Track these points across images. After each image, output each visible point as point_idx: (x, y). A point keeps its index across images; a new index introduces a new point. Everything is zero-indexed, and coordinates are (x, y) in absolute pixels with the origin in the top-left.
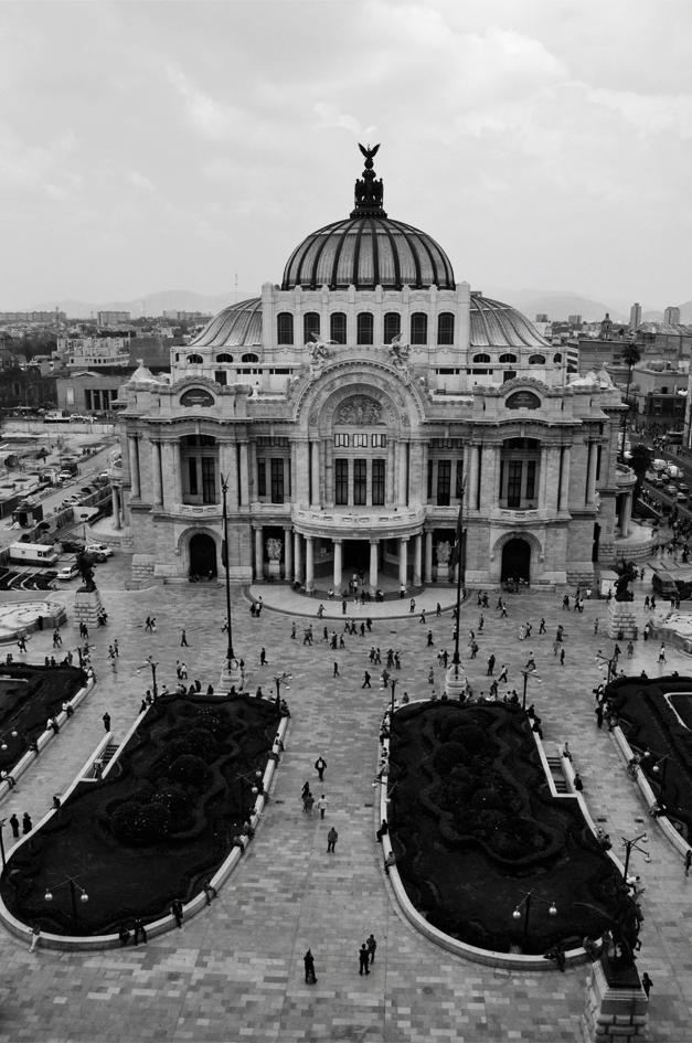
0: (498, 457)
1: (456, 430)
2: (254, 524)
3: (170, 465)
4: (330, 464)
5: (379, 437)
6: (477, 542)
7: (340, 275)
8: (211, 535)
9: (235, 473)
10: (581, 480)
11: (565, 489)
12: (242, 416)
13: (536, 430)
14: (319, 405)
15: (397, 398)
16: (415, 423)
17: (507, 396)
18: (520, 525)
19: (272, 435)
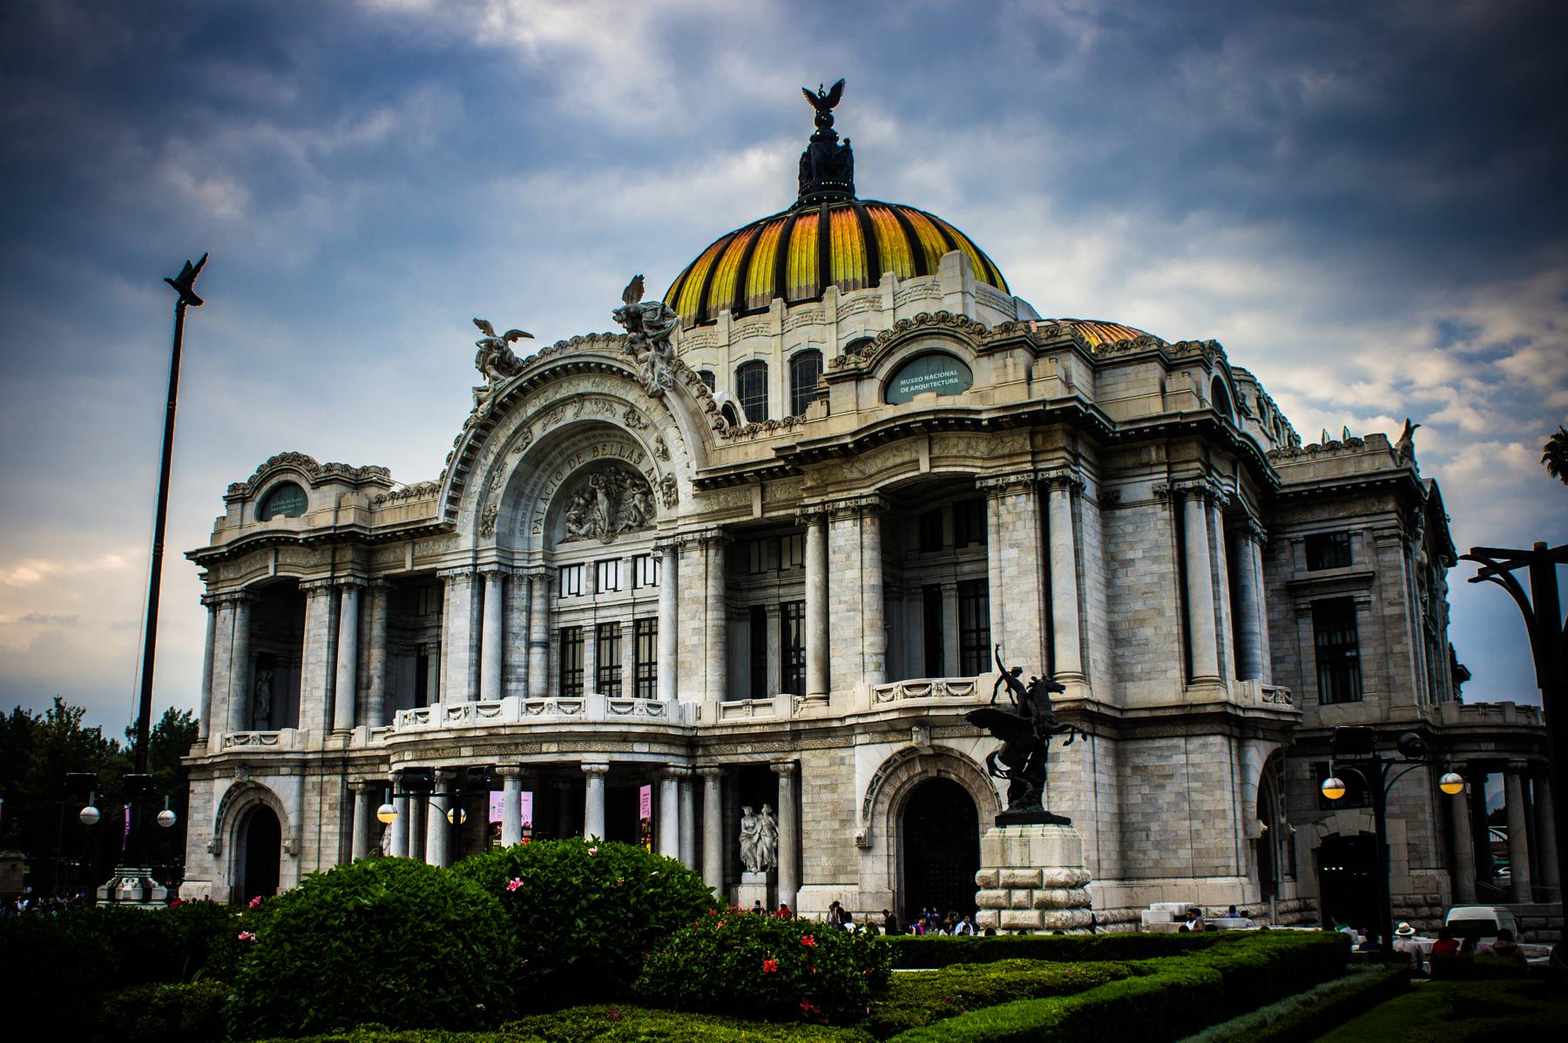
0: (870, 538)
1: (780, 492)
2: (351, 779)
3: (225, 651)
4: (538, 634)
5: (650, 562)
6: (826, 796)
7: (713, 303)
8: (272, 804)
9: (324, 654)
10: (1160, 612)
11: (1064, 608)
12: (348, 518)
13: (962, 445)
14: (500, 491)
15: (653, 444)
16: (686, 489)
17: (882, 373)
18: (918, 720)
19: (408, 567)
